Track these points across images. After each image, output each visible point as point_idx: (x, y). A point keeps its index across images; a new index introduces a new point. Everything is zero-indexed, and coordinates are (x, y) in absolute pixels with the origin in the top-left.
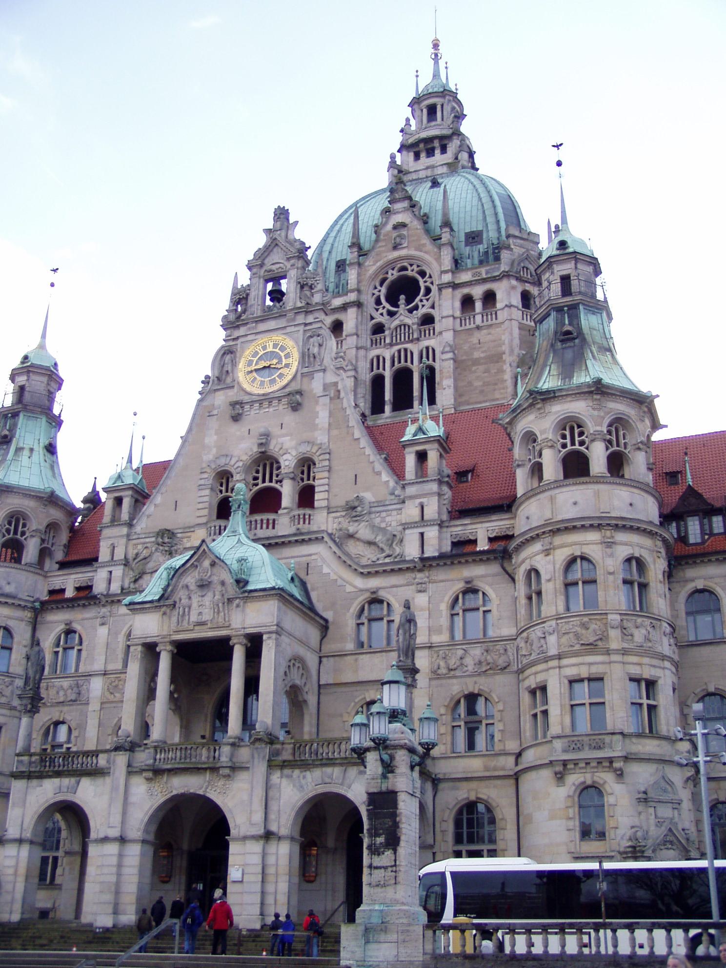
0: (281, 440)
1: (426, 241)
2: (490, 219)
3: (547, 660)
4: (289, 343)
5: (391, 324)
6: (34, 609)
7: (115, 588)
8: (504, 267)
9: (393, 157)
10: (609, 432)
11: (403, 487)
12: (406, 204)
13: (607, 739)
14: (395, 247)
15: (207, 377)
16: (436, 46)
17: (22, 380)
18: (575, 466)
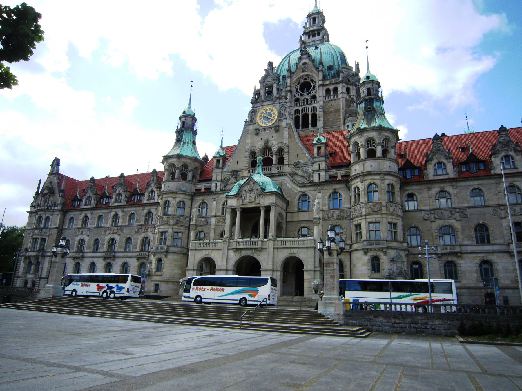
0: (272, 142)
1: (314, 69)
3: (361, 216)
4: (274, 109)
6: (192, 196)
7: (218, 189)
8: (340, 79)
9: (301, 37)
10: (383, 142)
11: (313, 159)
12: (307, 56)
13: (381, 242)
14: (303, 71)
15: (246, 120)
17: (183, 119)
18: (371, 154)
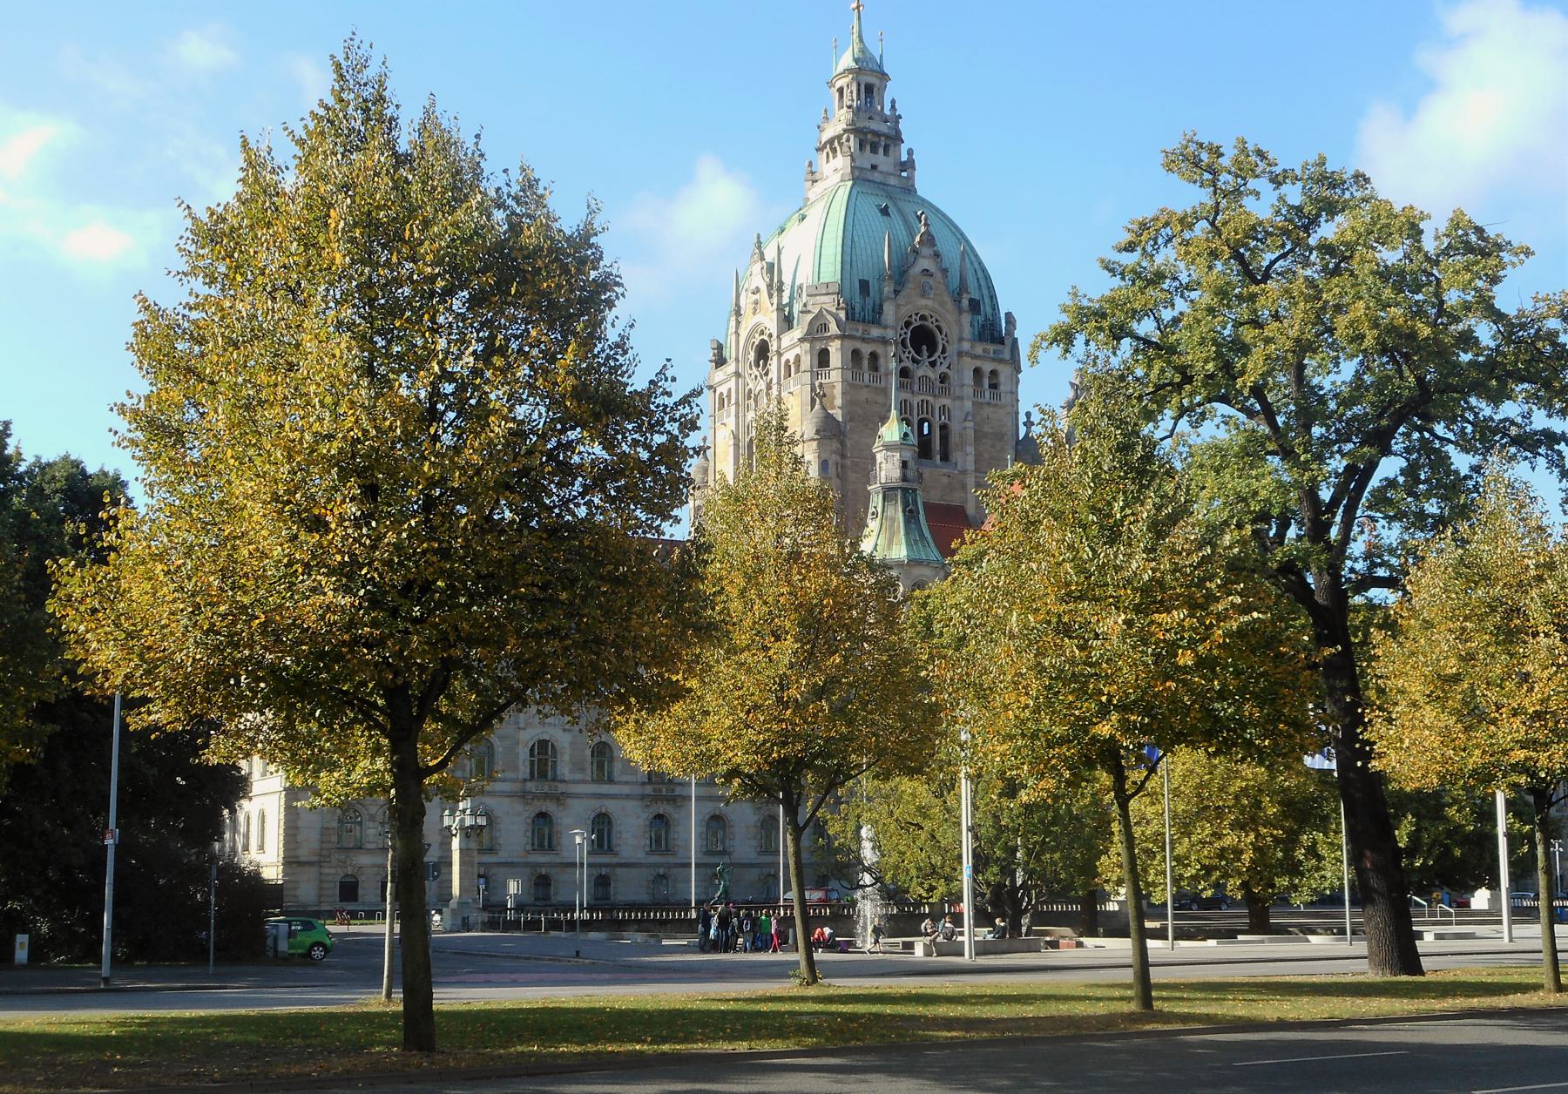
1: (947, 299)
2: (985, 292)
14: (924, 294)
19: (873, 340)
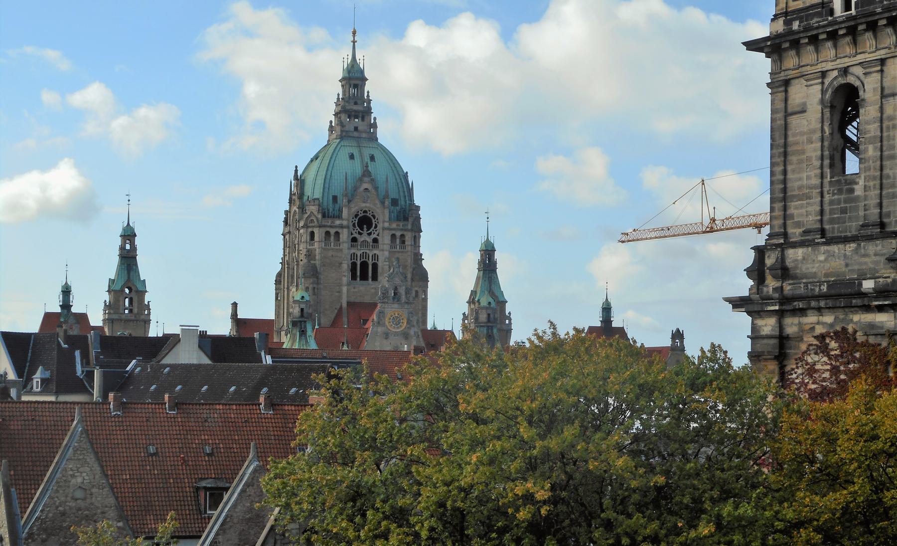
1: (377, 202)
2: (402, 194)
5: (361, 239)
16: (354, 33)
19: (336, 227)
